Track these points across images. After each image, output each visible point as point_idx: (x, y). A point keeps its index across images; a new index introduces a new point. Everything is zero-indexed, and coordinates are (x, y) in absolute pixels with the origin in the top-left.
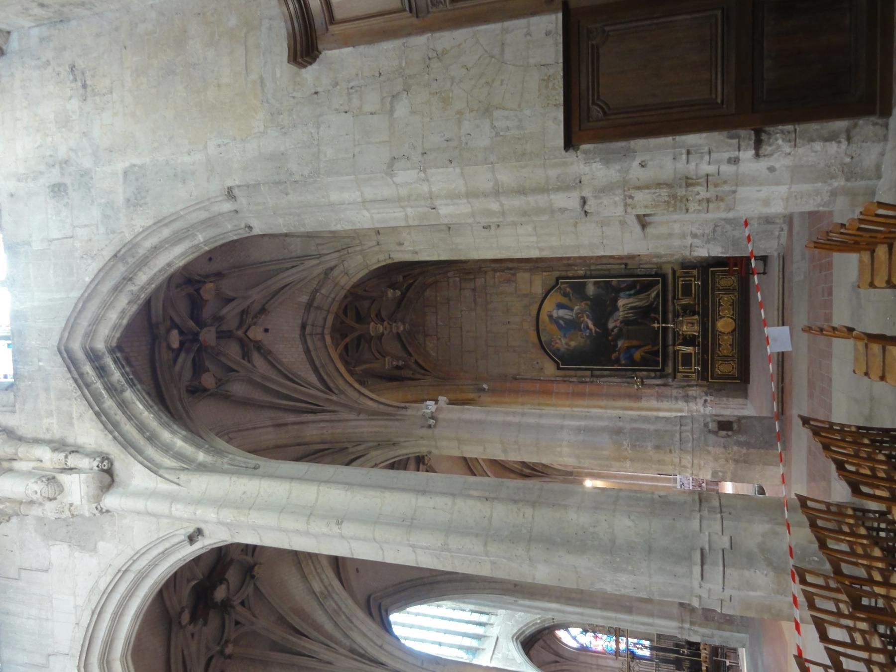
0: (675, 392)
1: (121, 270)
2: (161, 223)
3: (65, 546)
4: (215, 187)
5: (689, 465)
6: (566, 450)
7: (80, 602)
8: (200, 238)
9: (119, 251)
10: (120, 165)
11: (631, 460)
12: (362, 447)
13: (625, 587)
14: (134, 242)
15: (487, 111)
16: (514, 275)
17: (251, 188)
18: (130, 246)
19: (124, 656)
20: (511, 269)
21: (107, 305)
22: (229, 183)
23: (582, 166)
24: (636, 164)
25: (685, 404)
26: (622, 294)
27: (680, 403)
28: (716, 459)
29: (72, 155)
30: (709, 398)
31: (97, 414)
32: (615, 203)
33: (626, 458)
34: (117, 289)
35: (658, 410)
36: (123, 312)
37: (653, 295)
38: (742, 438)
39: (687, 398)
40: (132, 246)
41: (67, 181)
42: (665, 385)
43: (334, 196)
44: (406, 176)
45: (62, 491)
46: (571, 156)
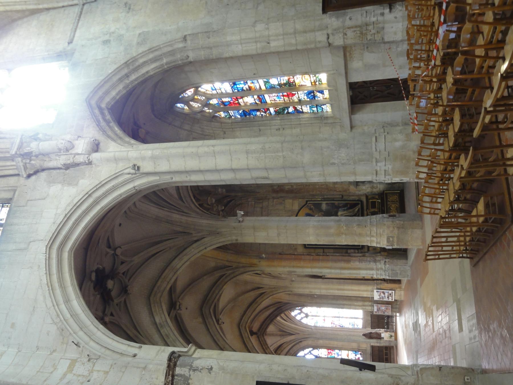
0: (369, 259)
1: (126, 71)
2: (151, 50)
3: (59, 186)
4: (180, 35)
5: (375, 235)
6: (311, 231)
7: (59, 211)
8: (165, 61)
9: (128, 61)
10: (138, 32)
11: (345, 234)
12: (200, 234)
13: (343, 160)
14: (136, 58)
15: (294, 5)
16: (284, 200)
17: (195, 35)
18: (134, 59)
19: (71, 250)
20: (282, 197)
21: (113, 87)
22: (186, 33)
23: (328, 19)
24: (348, 18)
25: (374, 264)
26: (340, 209)
27: (372, 263)
28: (388, 227)
29: (117, 30)
30: (387, 260)
31: (97, 125)
32: (340, 37)
33: (342, 234)
34: (121, 80)
35: (360, 269)
36: (119, 92)
37: (356, 210)
38: (400, 219)
39: (375, 261)
40: (134, 60)
41: (112, 39)
42: (364, 256)
43: (229, 38)
44: (260, 27)
45: (73, 147)
46: (325, 16)
